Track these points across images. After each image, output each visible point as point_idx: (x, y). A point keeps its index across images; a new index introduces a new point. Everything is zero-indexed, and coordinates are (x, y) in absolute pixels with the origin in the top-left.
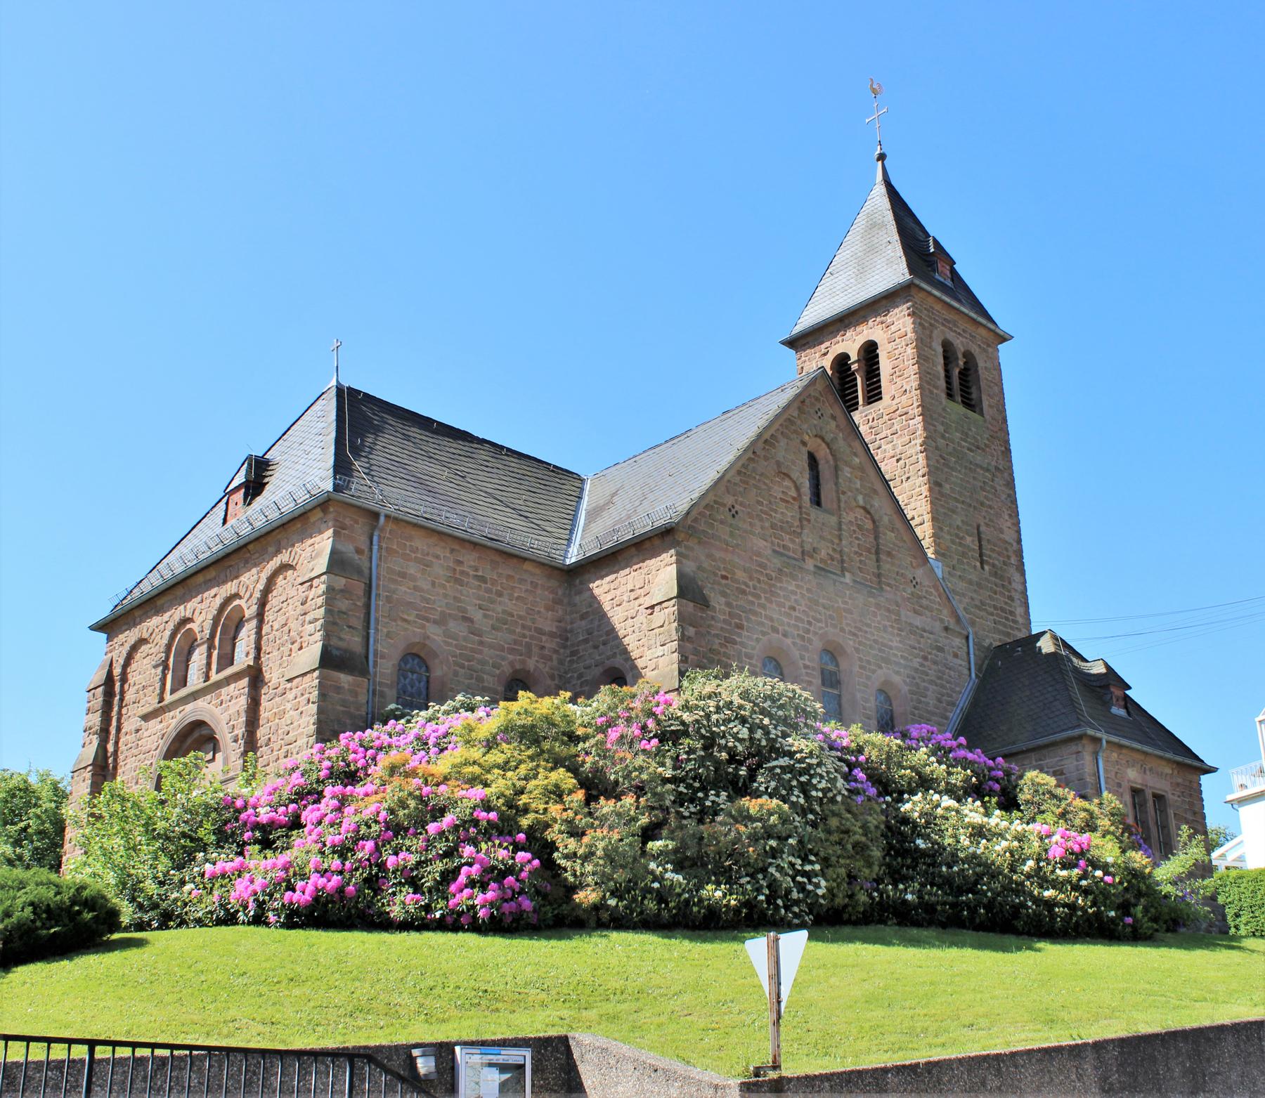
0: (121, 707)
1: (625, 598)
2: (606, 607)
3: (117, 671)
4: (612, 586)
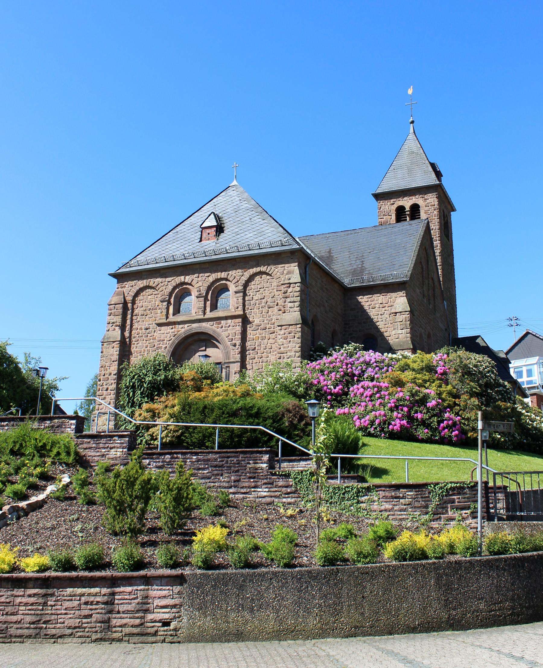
0: (132, 316)
1: (377, 306)
2: (366, 307)
3: (129, 298)
4: (369, 300)
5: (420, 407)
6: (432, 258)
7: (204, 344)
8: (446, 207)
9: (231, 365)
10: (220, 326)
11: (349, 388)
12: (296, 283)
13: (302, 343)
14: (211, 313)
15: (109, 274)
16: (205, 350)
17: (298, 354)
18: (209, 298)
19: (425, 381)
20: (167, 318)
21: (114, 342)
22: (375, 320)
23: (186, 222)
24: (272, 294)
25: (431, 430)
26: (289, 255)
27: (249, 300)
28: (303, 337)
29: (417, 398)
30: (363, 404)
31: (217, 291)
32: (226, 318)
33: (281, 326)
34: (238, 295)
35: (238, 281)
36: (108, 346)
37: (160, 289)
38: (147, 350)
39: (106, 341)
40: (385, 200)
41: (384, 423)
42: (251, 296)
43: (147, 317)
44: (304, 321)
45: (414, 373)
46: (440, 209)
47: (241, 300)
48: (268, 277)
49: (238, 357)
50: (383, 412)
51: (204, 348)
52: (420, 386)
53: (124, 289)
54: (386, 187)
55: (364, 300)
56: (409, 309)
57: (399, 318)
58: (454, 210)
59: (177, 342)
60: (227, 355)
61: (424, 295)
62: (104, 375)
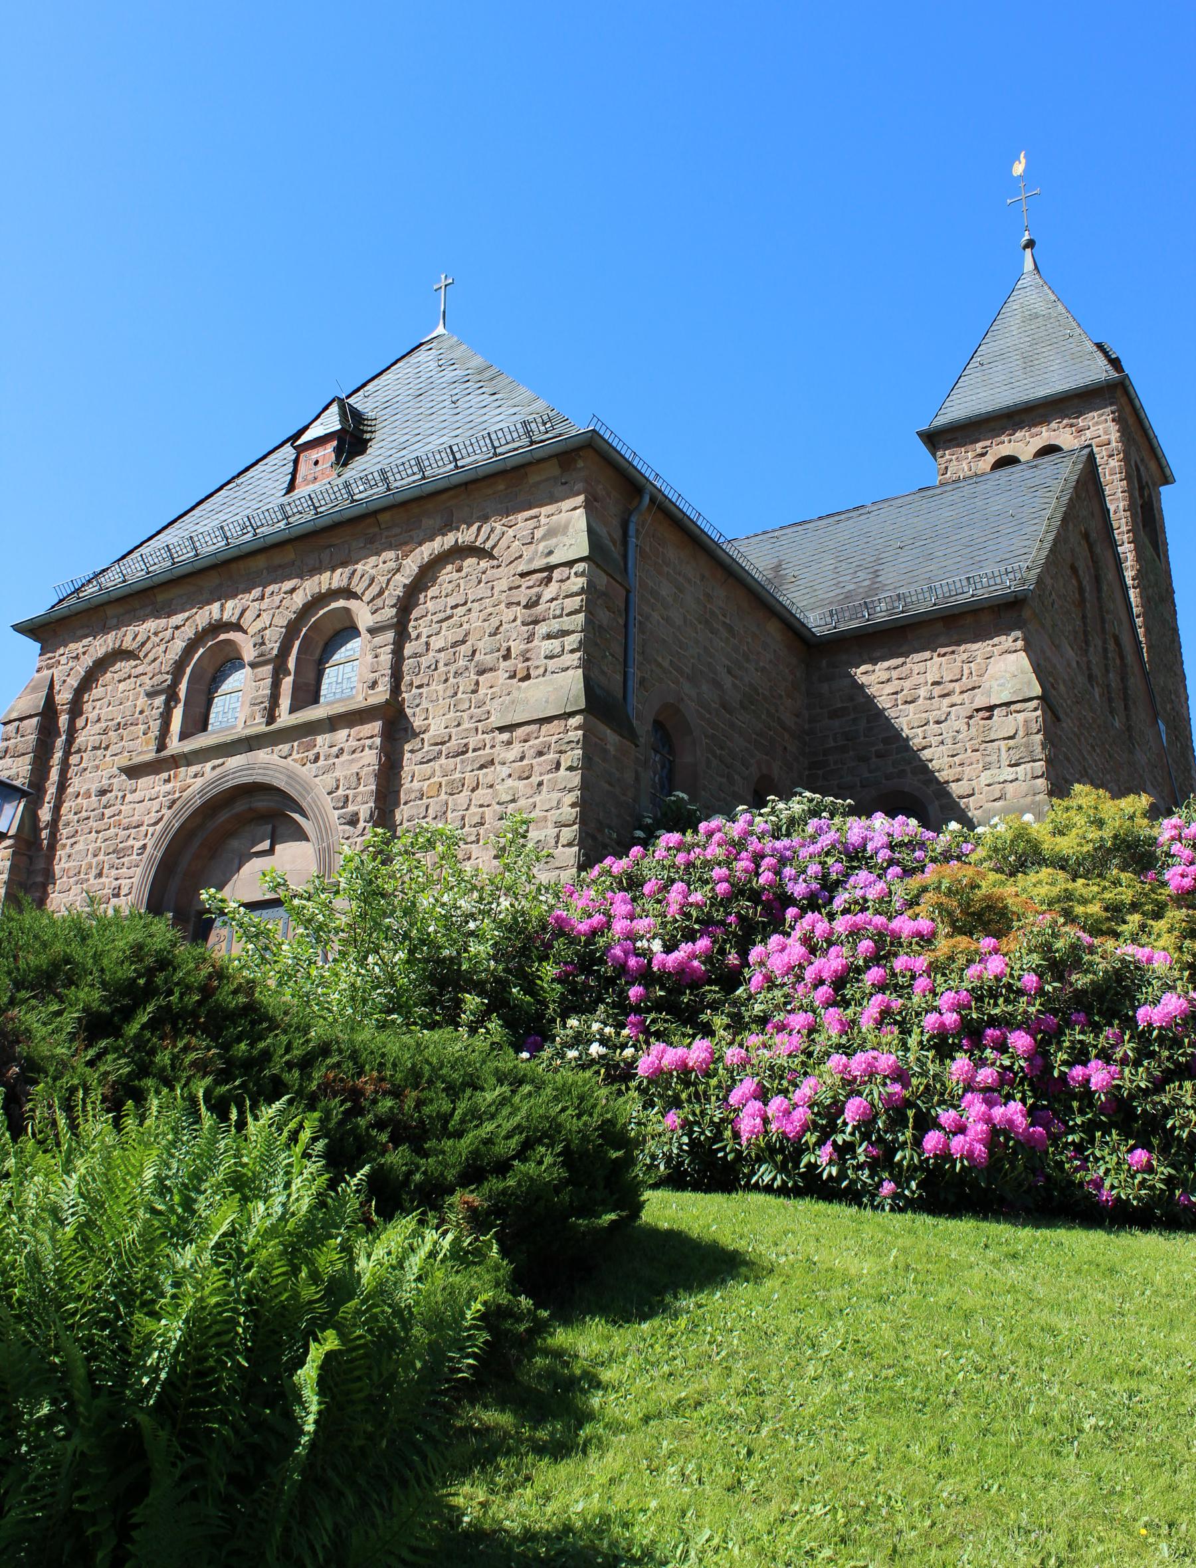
0: (67, 753)
1: (923, 692)
2: (883, 702)
3: (64, 697)
4: (895, 674)
5: (1097, 1029)
6: (1111, 575)
8: (1147, 467)
10: (311, 755)
11: (744, 954)
12: (570, 564)
13: (585, 786)
14: (294, 716)
15: (18, 628)
17: (568, 834)
18: (291, 664)
19: (1116, 911)
22: (916, 743)
24: (494, 622)
25: (1164, 1150)
26: (556, 471)
28: (588, 764)
29: (1080, 980)
30: (798, 1020)
31: (318, 639)
34: (380, 639)
35: (381, 593)
37: (151, 656)
40: (959, 446)
41: (897, 1121)
42: (423, 639)
43: (108, 753)
44: (601, 704)
45: (1061, 875)
46: (1126, 453)
47: (386, 658)
48: (484, 564)
50: (886, 1061)
51: (265, 845)
52: (1095, 930)
54: (959, 408)
55: (877, 679)
56: (1037, 690)
57: (1003, 724)
58: (1167, 479)
61: (1090, 678)
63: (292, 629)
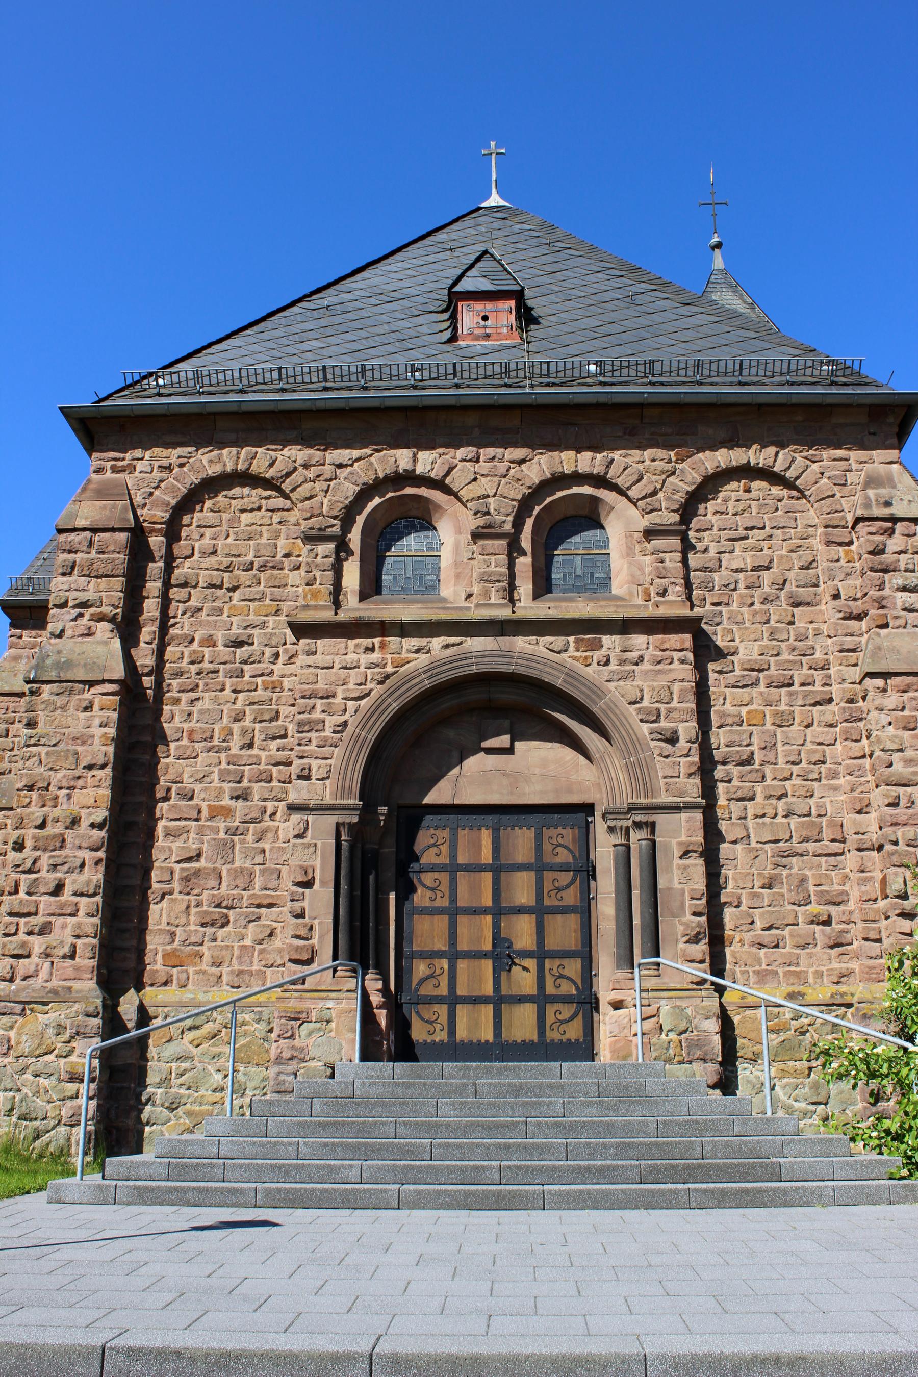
3: (155, 514)
7: (506, 723)
9: (662, 820)
16: (510, 751)
18: (526, 541)
20: (337, 605)
21: (91, 684)
23: (348, 284)
27: (704, 569)
31: (559, 522)
32: (626, 626)
33: (886, 675)
35: (654, 493)
36: (60, 701)
37: (303, 491)
38: (244, 732)
39: (53, 675)
42: (712, 553)
43: (236, 595)
47: (673, 561)
48: (776, 491)
49: (692, 788)
51: (503, 740)
53: (130, 480)
59: (395, 706)
60: (639, 772)
62: (42, 826)
63: (524, 507)
